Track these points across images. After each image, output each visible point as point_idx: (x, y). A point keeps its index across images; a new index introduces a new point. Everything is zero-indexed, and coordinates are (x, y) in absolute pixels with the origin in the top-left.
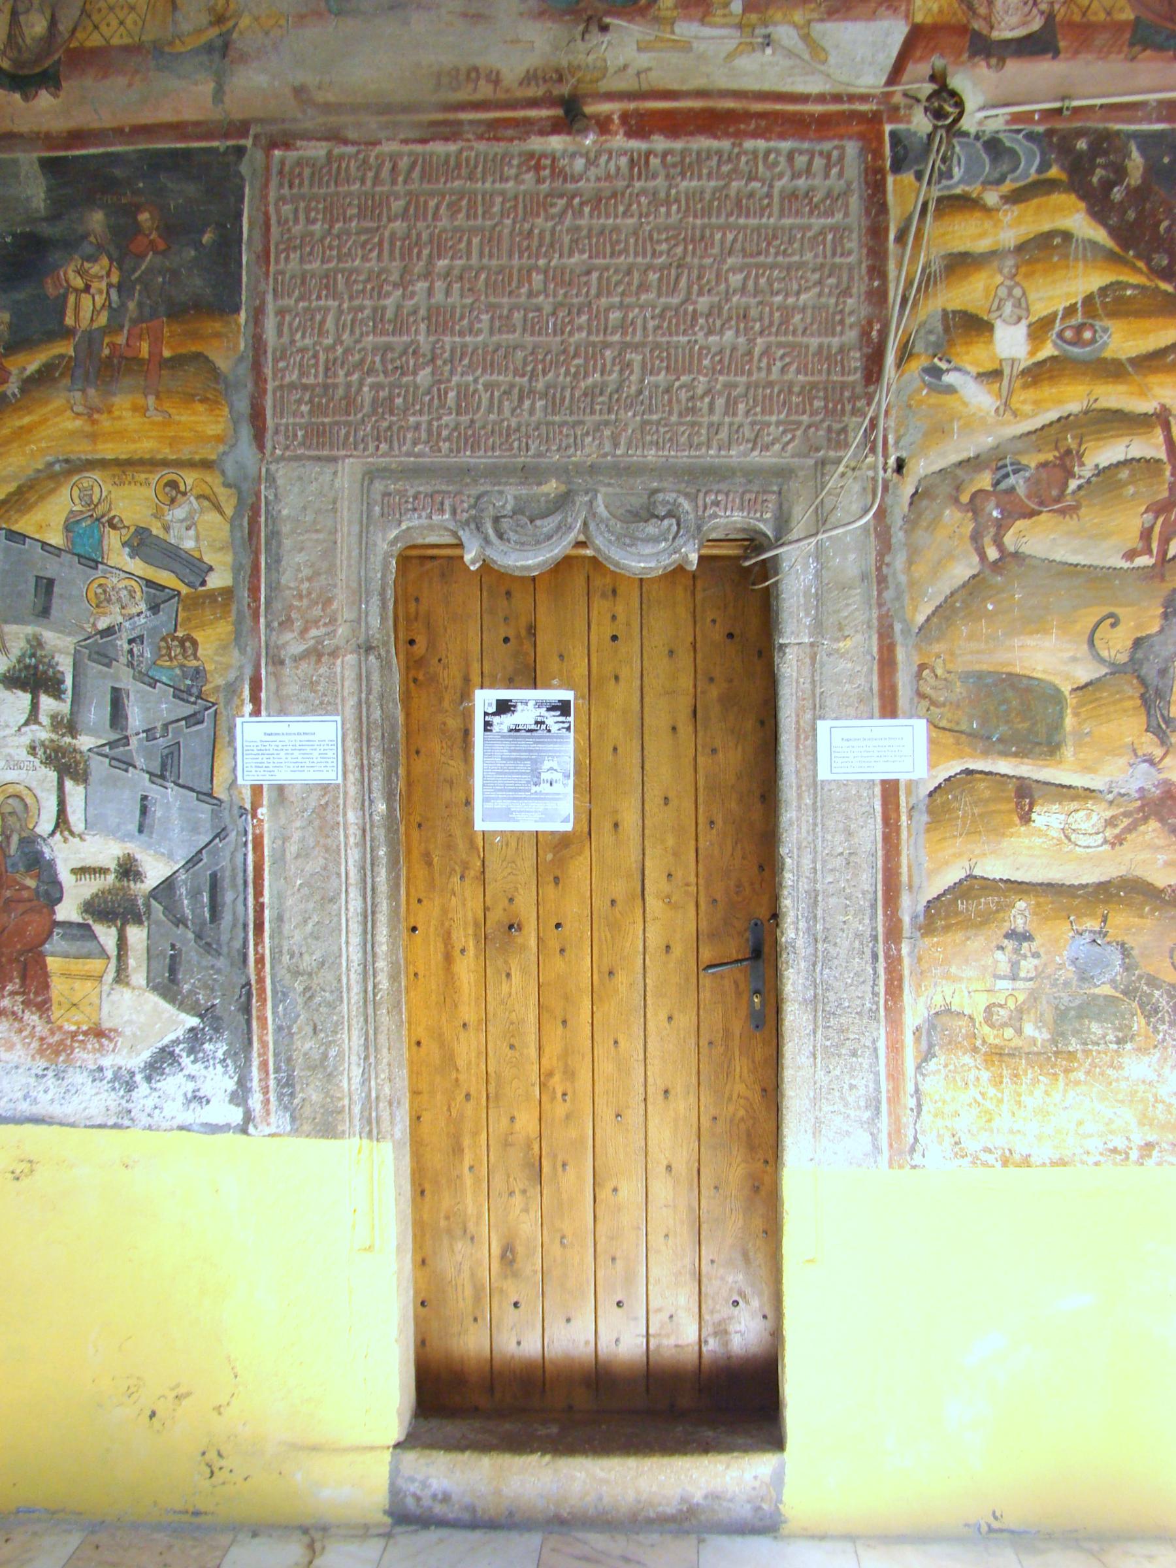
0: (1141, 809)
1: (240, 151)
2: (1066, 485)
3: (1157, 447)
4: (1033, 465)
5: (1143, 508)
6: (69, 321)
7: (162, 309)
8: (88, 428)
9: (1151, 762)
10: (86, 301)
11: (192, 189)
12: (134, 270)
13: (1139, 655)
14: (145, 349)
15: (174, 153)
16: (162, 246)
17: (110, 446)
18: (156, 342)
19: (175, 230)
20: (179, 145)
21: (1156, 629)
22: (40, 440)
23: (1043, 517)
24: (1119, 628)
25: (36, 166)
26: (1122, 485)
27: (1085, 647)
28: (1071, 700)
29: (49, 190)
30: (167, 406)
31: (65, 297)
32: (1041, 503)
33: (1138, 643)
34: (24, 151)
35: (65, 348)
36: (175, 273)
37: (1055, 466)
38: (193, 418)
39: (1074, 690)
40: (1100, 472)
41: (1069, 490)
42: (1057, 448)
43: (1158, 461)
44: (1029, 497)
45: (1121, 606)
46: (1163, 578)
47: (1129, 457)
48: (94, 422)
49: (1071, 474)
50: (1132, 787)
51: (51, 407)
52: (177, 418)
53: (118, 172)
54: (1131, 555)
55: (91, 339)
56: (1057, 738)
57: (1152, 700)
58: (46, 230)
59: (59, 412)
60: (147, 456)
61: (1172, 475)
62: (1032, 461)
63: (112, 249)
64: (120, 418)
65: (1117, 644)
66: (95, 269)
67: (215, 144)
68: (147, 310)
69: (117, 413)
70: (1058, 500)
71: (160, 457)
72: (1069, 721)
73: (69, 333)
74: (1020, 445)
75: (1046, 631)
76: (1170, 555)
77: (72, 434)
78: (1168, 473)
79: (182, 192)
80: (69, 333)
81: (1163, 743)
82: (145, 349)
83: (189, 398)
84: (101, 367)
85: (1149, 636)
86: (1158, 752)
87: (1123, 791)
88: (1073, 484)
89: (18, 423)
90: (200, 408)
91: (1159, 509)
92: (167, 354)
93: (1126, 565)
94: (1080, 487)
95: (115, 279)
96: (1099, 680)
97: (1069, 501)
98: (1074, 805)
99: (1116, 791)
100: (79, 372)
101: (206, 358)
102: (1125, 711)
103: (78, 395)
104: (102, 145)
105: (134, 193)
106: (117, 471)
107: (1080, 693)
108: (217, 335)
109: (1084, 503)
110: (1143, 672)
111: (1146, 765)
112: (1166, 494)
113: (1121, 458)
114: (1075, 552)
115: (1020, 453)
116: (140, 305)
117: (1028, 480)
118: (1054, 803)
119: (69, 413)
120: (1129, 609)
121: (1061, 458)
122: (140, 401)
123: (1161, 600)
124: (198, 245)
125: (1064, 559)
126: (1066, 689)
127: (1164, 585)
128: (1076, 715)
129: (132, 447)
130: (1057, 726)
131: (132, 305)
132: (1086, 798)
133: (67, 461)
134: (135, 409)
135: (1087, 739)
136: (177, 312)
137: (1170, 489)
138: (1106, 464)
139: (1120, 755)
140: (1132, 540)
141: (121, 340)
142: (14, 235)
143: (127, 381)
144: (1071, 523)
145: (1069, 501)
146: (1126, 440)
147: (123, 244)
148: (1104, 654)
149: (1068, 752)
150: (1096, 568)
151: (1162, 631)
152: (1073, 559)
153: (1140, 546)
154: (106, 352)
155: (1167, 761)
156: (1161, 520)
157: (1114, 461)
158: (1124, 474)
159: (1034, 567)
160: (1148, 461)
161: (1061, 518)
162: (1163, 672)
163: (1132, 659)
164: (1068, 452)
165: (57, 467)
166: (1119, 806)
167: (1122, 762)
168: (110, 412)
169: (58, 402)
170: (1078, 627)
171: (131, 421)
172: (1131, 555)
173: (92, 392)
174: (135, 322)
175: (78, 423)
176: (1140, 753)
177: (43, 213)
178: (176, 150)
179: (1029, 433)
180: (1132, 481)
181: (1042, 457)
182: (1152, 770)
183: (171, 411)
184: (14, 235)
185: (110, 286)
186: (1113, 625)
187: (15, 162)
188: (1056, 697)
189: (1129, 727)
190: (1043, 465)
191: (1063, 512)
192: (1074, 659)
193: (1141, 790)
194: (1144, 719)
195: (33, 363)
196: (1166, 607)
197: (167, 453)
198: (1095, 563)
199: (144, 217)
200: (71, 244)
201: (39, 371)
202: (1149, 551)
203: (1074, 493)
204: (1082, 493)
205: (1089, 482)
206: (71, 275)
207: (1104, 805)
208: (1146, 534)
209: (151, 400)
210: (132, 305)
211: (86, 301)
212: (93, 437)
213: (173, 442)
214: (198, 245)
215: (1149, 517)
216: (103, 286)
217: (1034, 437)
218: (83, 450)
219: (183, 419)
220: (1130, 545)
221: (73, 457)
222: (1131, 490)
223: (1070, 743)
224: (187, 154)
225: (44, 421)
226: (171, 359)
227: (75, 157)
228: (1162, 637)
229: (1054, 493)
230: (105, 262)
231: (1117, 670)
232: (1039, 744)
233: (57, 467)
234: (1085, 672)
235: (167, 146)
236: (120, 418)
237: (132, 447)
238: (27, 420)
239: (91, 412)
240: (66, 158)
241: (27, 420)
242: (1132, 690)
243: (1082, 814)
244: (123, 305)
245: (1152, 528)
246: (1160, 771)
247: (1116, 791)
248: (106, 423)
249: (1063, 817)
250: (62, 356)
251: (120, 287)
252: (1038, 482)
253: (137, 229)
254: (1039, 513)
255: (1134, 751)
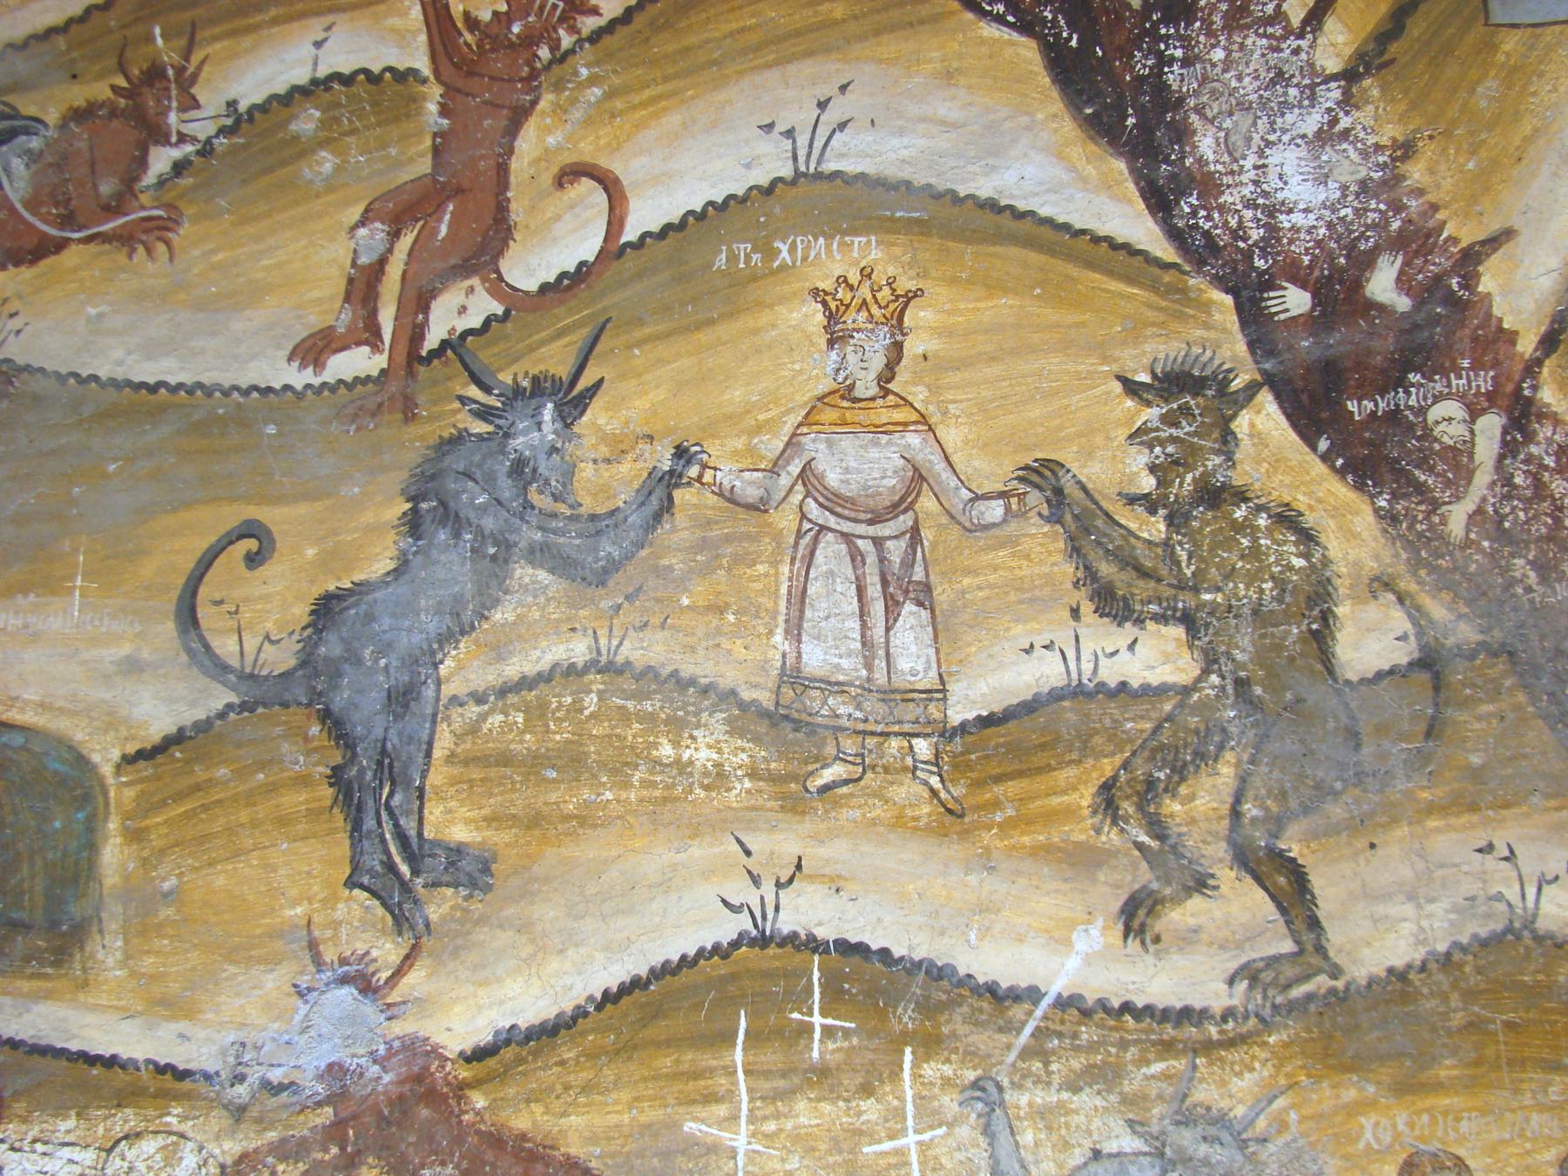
0: (334, 1133)
2: (143, 163)
3: (402, 38)
4: (52, 117)
5: (355, 213)
9: (366, 986)
13: (331, 647)
21: (384, 565)
23: (71, 257)
24: (271, 569)
26: (302, 150)
27: (168, 628)
28: (121, 792)
32: (68, 221)
33: (327, 609)
37: (114, 113)
39: (129, 760)
40: (239, 120)
41: (150, 178)
42: (123, 69)
43: (404, 76)
44: (33, 204)
45: (280, 500)
46: (410, 415)
47: (322, 72)
49: (160, 135)
50: (306, 1063)
54: (314, 350)
56: (76, 910)
57: (369, 787)
61: (444, 111)
62: (49, 105)
65: (263, 617)
70: (112, 209)
72: (113, 855)
74: (21, 66)
75: (52, 586)
76: (432, 340)
78: (432, 107)
81: (401, 921)
85: (361, 588)
86: (388, 952)
87: (276, 1075)
88: (161, 160)
91: (402, 211)
93: (299, 377)
94: (179, 167)
96: (204, 727)
97: (146, 207)
98: (126, 1119)
99: (254, 1075)
102: (283, 821)
107: (145, 769)
109: (190, 211)
110: (339, 701)
111: (347, 993)
112: (425, 166)
113: (301, 76)
114: (151, 351)
115: (17, 87)
117: (33, 157)
118: (60, 1111)
120: (303, 509)
121: (131, 94)
123: (398, 478)
125: (120, 374)
126: (105, 756)
127: (413, 430)
128: (134, 836)
130: (77, 871)
132: (164, 1097)
135: (167, 912)
137: (436, 151)
138: (258, 98)
139: (272, 961)
140: (323, 303)
144: (149, 268)
145: (146, 207)
146: (314, 28)
148: (226, 647)
149: (108, 952)
150: (209, 391)
151: (397, 572)
152: (147, 372)
153: (344, 319)
155: (415, 979)
156: (406, 241)
157: (280, 88)
158: (307, 121)
159: (37, 399)
160: (373, 78)
161: (121, 257)
162: (402, 699)
163: (307, 661)
164: (155, 74)
166: (263, 1123)
167: (274, 981)
170: (148, 569)
172: (314, 350)
176: (329, 955)
179: (51, 32)
180: (327, 139)
181: (79, 95)
182: (369, 1009)
186: (253, 560)
188: (75, 783)
189: (300, 873)
190: (82, 115)
191: (126, 239)
192: (132, 667)
193: (334, 1070)
194: (342, 847)
196: (414, 499)
198: (207, 379)
202: (372, 336)
203: (162, 182)
204: (186, 181)
205: (207, 150)
207: (218, 1119)
208: (363, 286)
215: (373, 237)
217: (61, 42)
220: (315, 320)
222: (327, 162)
223: (112, 926)
228: (401, 589)
229: (107, 188)
231: (260, 694)
232: (25, 927)
234: (159, 710)
242: (305, 756)
243: (149, 1146)
245: (382, 262)
246: (391, 1012)
247: (254, 1075)
249: (88, 1157)
252: (63, 162)
254: (60, 246)
255: (313, 945)
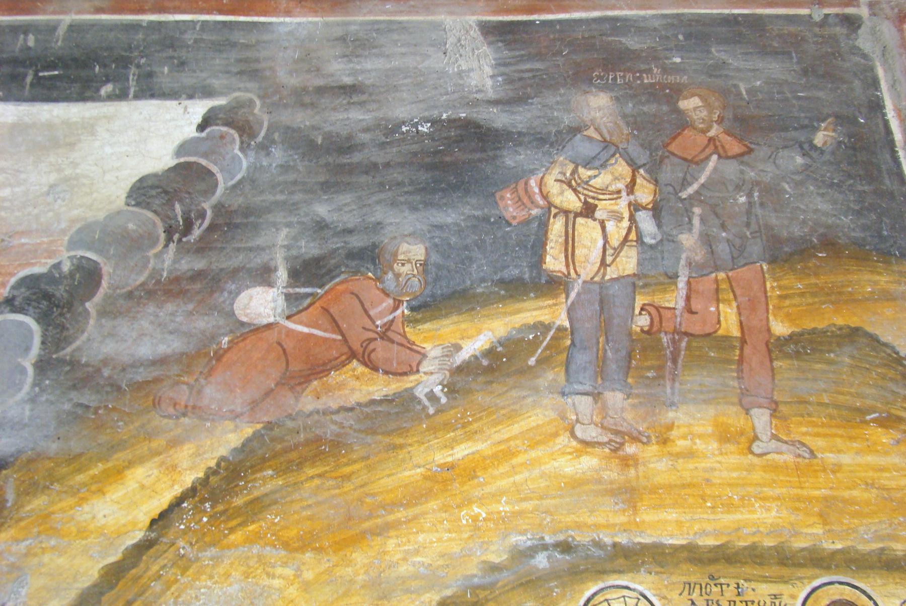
1: (852, 23)
6: (554, 262)
7: (756, 248)
8: (612, 474)
10: (588, 231)
11: (775, 68)
12: (685, 183)
14: (729, 320)
15: (731, 21)
16: (735, 148)
17: (672, 515)
18: (753, 306)
19: (750, 125)
20: (736, 11)
22: (496, 496)
25: (475, 33)
29: (501, 63)
30: (800, 430)
31: (544, 226)
34: (451, 13)
35: (554, 313)
36: (771, 192)
38: (870, 459)
48: (627, 462)
51: (516, 429)
52: (831, 457)
53: (632, 42)
55: (603, 298)
58: (499, 118)
59: (538, 438)
60: (769, 542)
63: (634, 149)
64: (690, 454)
66: (602, 180)
67: (804, 11)
68: (723, 249)
69: (682, 444)
71: (799, 544)
73: (553, 285)
77: (576, 484)
79: (755, 74)
80: (553, 285)
82: (729, 320)
83: (854, 416)
84: (642, 353)
89: (441, 457)
90: (884, 437)
92: (780, 328)
95: (645, 194)
100: (581, 358)
101: (874, 340)
103: (585, 403)
104: (594, 8)
105: (665, 70)
106: (696, 575)
108: (887, 297)
116: (707, 240)
119: (564, 439)
122: (734, 417)
124: (808, 149)
129: (728, 519)
131: (688, 240)
133: (565, 547)
134: (725, 436)
136: (787, 254)
141: (674, 299)
142: (434, 122)
143: (695, 379)
147: (655, 140)
154: (643, 321)
165: (541, 561)
168: (664, 441)
169: (538, 415)
171: (720, 463)
173: (615, 398)
174: (699, 270)
175: (589, 462)
177: (491, 95)
178: (735, 17)
183: (817, 443)
184: (434, 122)
185: (635, 207)
187: (437, 26)
195: (477, 335)
197: (811, 534)
199: (689, 104)
200: (550, 141)
201: (490, 353)
206: (553, 187)
209: (761, 418)
210: (688, 240)
211: (588, 231)
212: (629, 495)
213: (828, 508)
214: (808, 149)
216: (622, 205)
218: (606, 524)
219: (846, 459)
221: (582, 538)
224: (756, 23)
225: (505, 454)
226: (791, 338)
227: (544, 23)
230: (622, 168)
233: (541, 561)
235: (715, 11)
236: (690, 454)
237: (728, 519)
238: (461, 451)
239: (618, 442)
240: (532, 22)
241: (461, 451)
244: (667, 240)
248: (656, 465)
250: (543, 327)
251: (656, 210)
253: (683, 123)
